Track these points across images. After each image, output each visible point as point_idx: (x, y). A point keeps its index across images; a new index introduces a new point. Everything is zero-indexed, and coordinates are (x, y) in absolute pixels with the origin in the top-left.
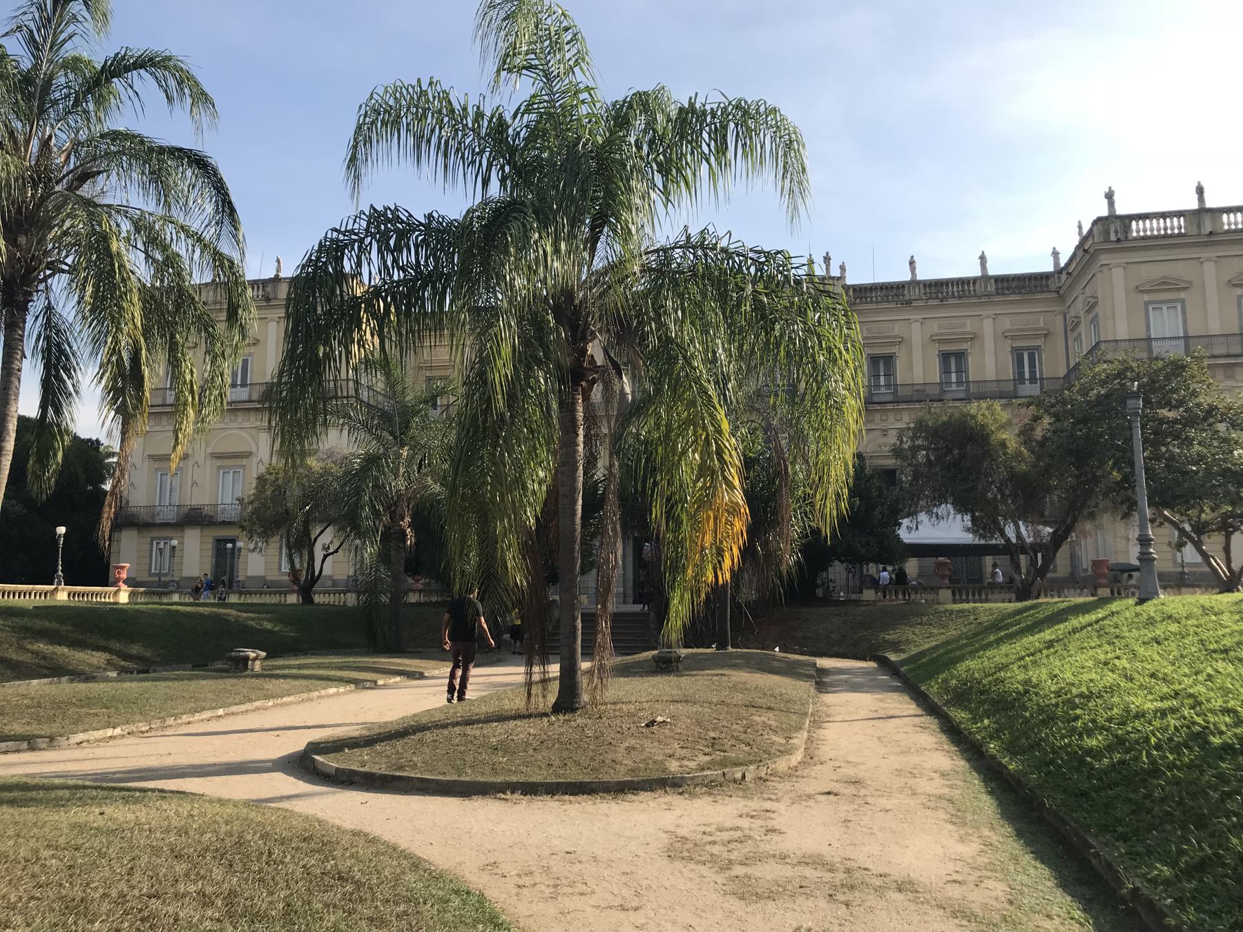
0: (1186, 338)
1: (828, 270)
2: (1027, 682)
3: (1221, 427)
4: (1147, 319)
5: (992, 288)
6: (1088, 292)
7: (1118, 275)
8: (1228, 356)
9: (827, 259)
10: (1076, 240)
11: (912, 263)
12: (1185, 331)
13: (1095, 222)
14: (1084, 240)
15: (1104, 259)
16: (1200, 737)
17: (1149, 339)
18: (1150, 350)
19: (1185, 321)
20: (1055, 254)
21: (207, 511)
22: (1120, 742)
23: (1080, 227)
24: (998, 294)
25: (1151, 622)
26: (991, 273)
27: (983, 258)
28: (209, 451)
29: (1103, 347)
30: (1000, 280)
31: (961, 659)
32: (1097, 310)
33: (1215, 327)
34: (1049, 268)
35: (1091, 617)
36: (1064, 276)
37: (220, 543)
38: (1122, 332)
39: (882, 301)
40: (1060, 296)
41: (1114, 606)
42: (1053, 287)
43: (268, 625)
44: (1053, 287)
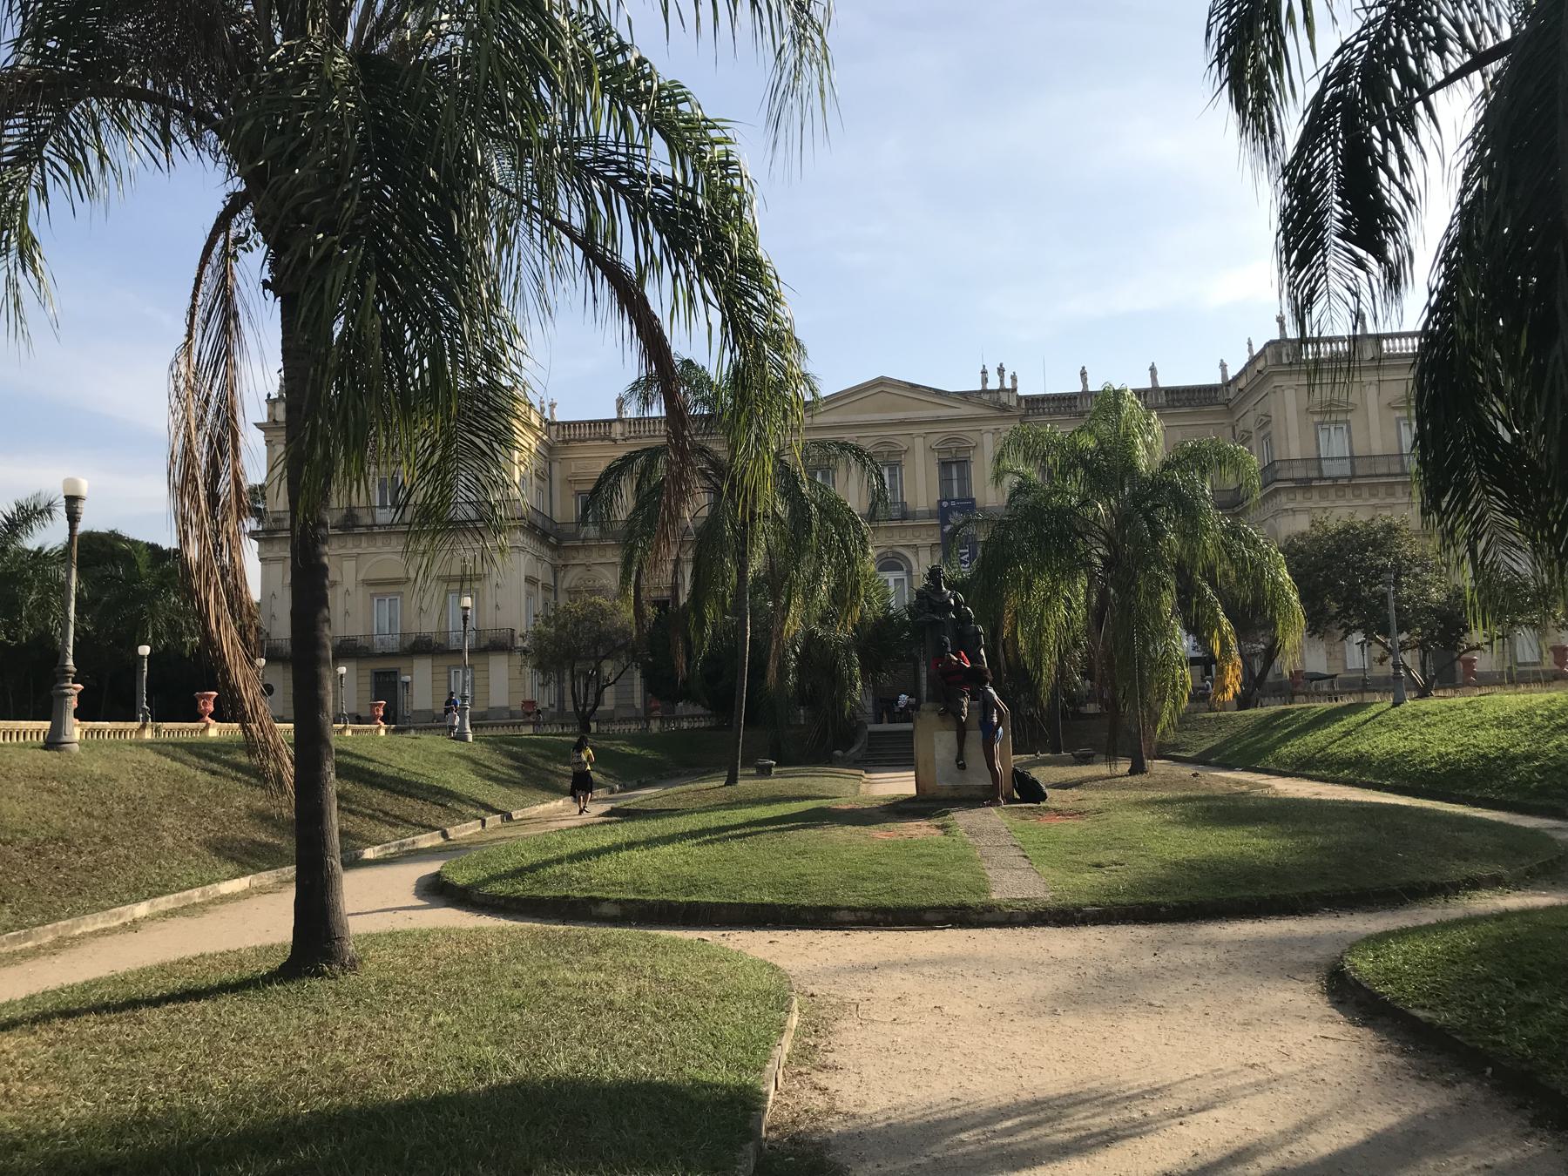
0: (1352, 457)
1: (1002, 381)
2: (1356, 751)
3: (1418, 570)
4: (1317, 439)
5: (1162, 400)
6: (1260, 409)
7: (1290, 395)
8: (1388, 475)
9: (1001, 371)
10: (1245, 359)
11: (1083, 374)
12: (1351, 451)
13: (1268, 344)
14: (1253, 360)
15: (1277, 381)
16: (1484, 756)
17: (1319, 459)
18: (1320, 469)
19: (1350, 438)
20: (1223, 366)
21: (361, 642)
22: (1445, 764)
23: (1250, 344)
24: (1168, 406)
25: (1415, 716)
26: (1162, 383)
27: (1153, 370)
28: (360, 577)
29: (1277, 465)
30: (1170, 391)
31: (1272, 748)
32: (1269, 428)
33: (1377, 449)
34: (1219, 381)
35: (1361, 717)
36: (1232, 389)
37: (377, 674)
38: (1295, 453)
39: (1055, 413)
40: (1229, 408)
41: (1374, 709)
42: (1221, 399)
43: (628, 750)
44: (1221, 397)
